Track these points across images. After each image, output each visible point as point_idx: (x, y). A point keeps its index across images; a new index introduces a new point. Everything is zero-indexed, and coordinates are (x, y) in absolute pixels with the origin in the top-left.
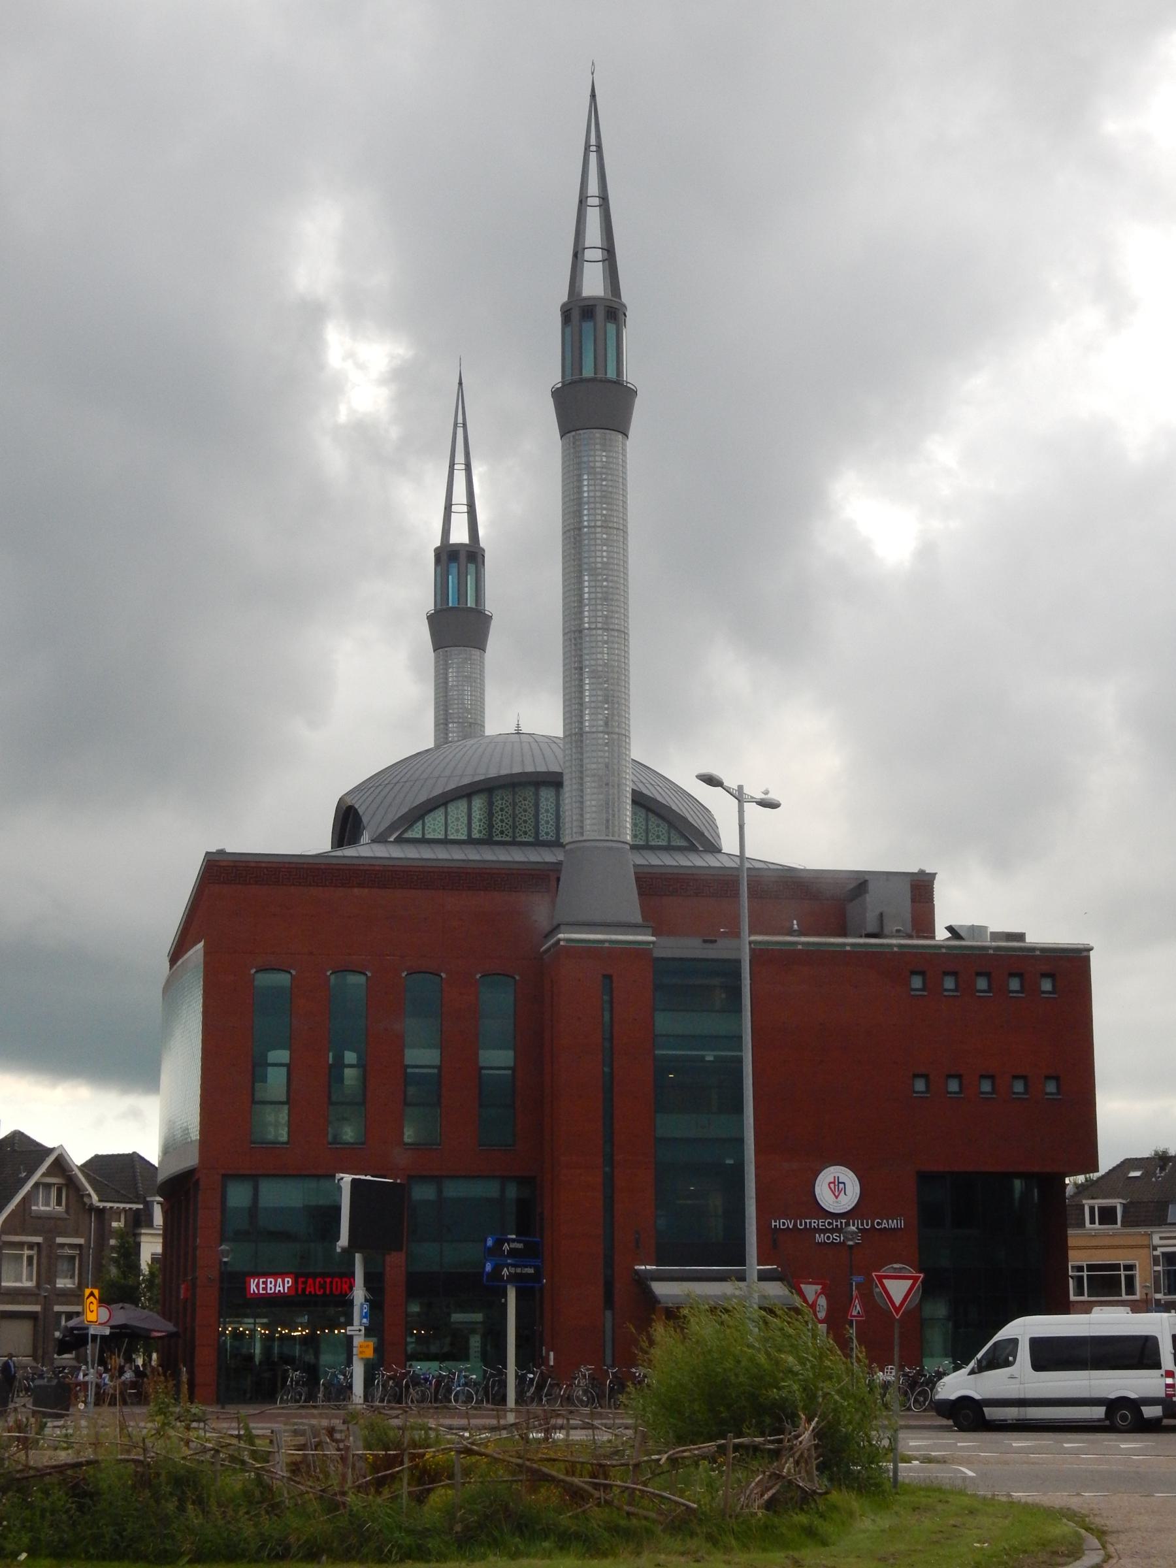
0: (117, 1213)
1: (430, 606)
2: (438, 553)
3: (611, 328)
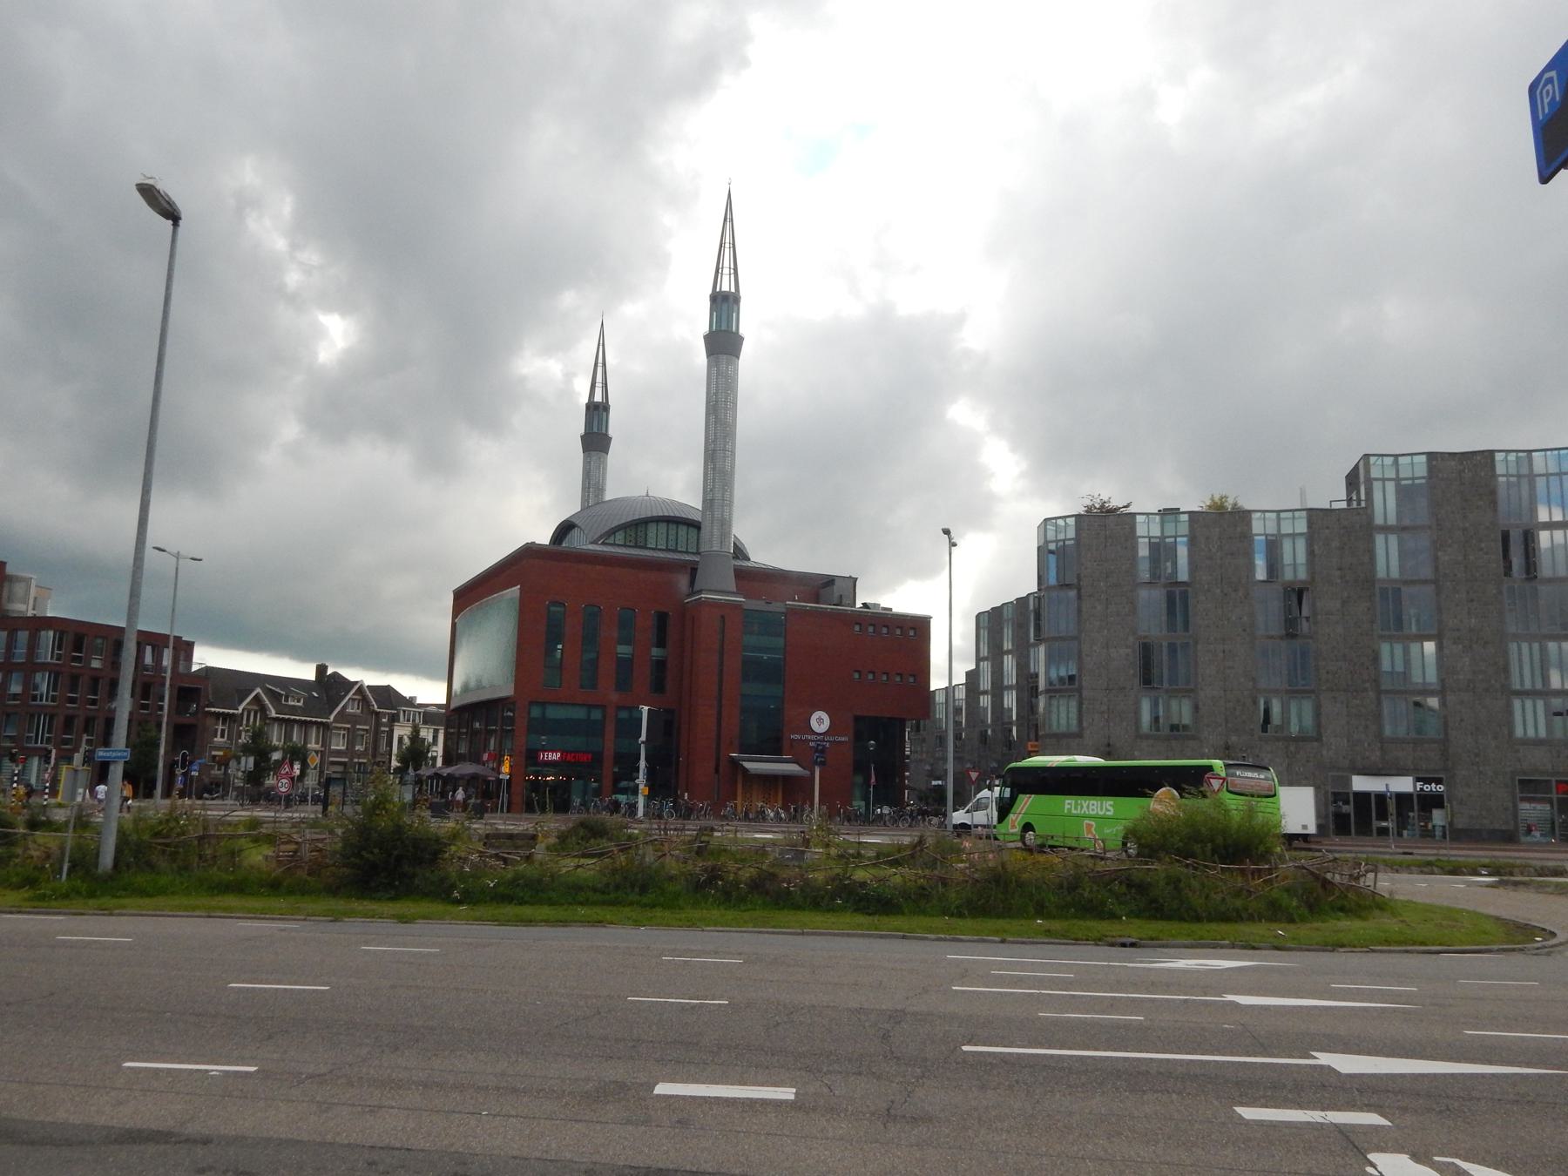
1: (582, 431)
2: (588, 406)
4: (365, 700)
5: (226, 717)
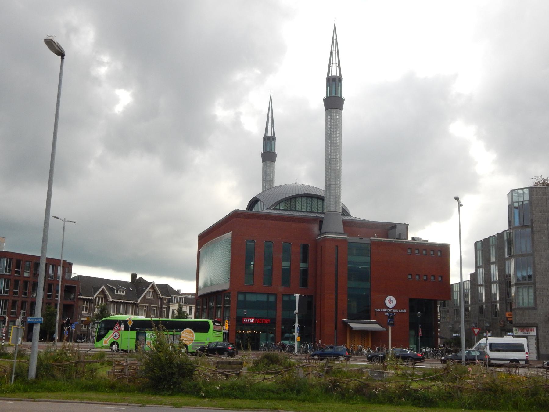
0: (165, 299)
3: (339, 84)
4: (155, 291)
5: (88, 301)
